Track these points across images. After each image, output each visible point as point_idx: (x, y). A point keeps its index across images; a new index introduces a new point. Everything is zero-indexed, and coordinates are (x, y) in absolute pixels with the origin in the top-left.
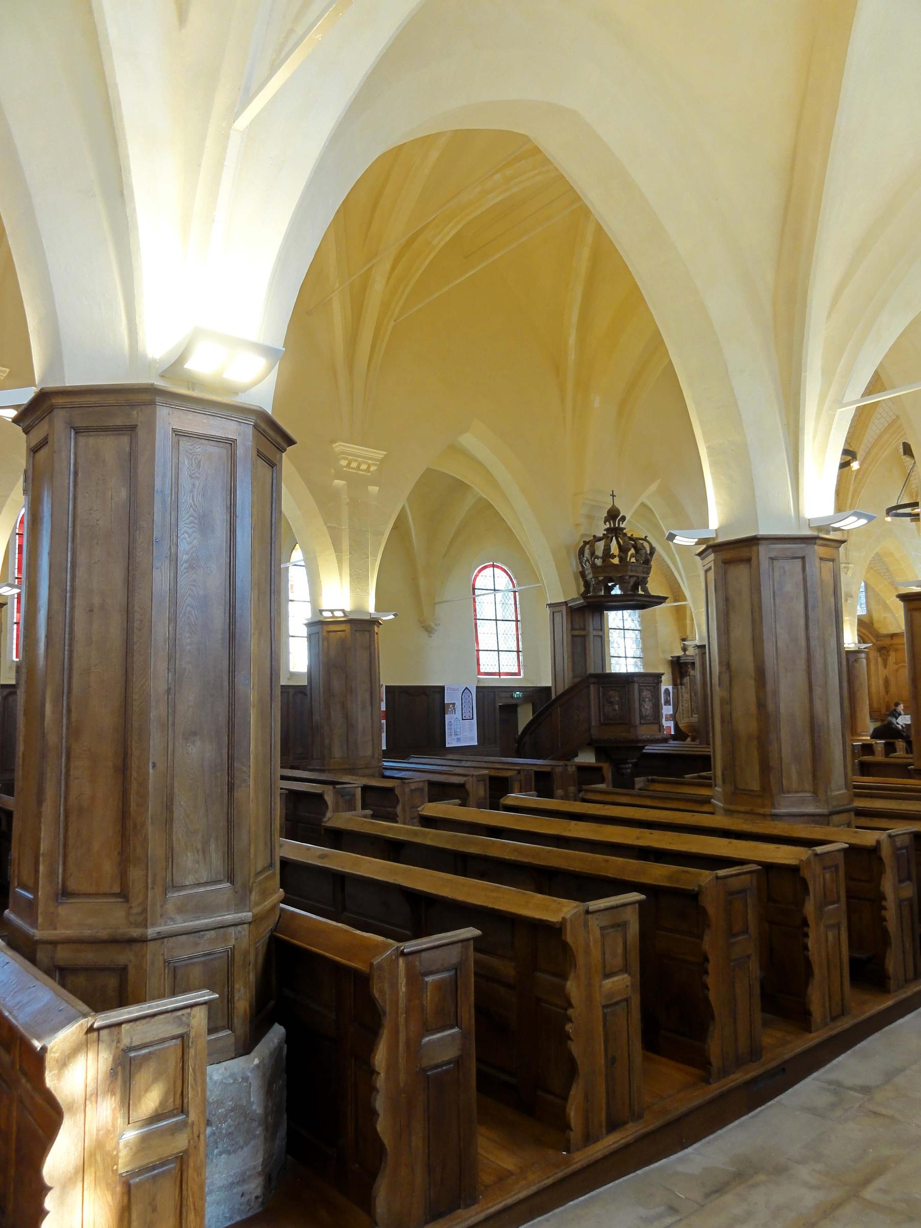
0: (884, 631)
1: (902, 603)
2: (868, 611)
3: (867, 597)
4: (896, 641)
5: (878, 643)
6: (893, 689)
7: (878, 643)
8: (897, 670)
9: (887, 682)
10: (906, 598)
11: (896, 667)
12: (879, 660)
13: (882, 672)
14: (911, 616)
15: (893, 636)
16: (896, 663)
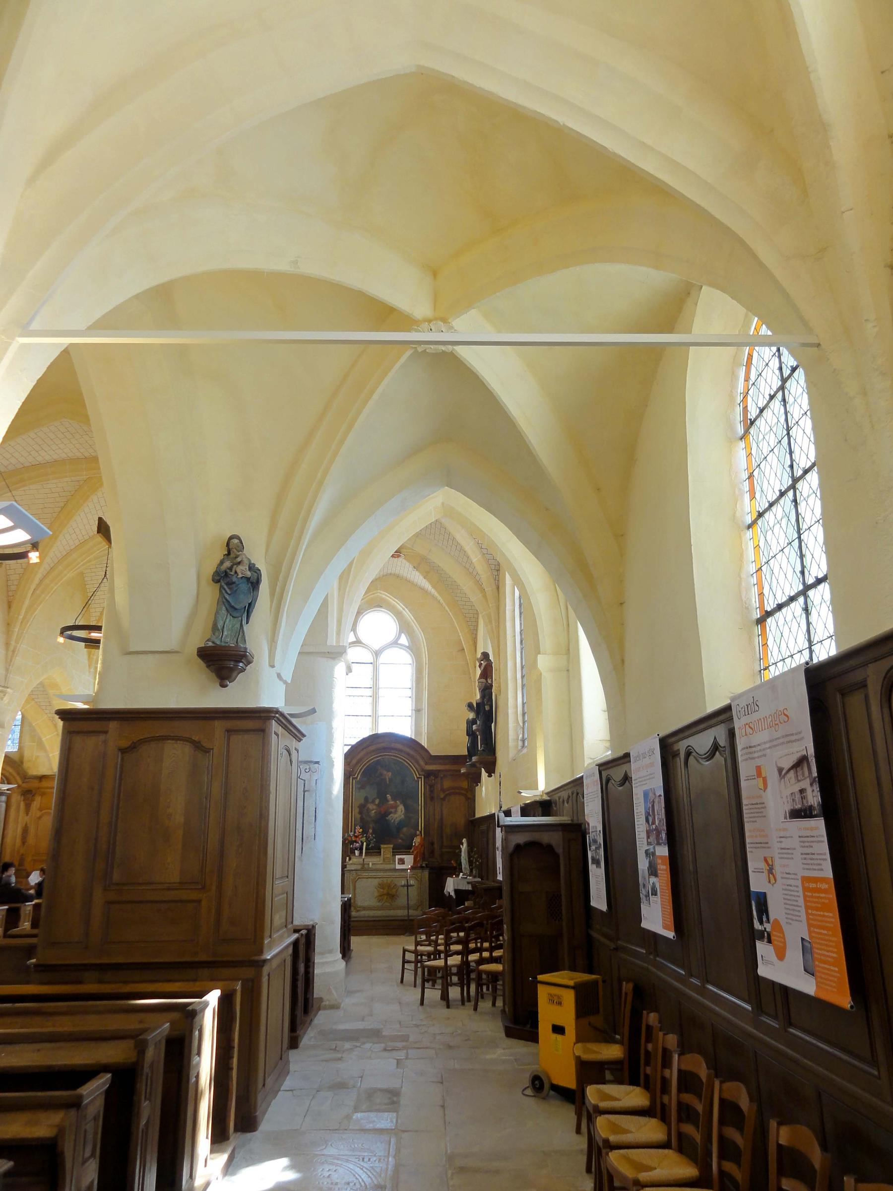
0: (34, 772)
1: (60, 723)
2: (20, 748)
3: (21, 732)
4: (44, 784)
5: (24, 785)
6: (31, 840)
7: (24, 785)
8: (40, 818)
9: (25, 831)
10: (66, 715)
11: (39, 814)
12: (22, 804)
13: (23, 819)
14: (70, 742)
15: (42, 778)
16: (40, 809)
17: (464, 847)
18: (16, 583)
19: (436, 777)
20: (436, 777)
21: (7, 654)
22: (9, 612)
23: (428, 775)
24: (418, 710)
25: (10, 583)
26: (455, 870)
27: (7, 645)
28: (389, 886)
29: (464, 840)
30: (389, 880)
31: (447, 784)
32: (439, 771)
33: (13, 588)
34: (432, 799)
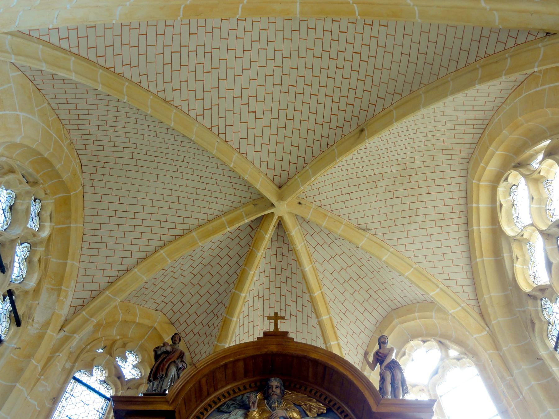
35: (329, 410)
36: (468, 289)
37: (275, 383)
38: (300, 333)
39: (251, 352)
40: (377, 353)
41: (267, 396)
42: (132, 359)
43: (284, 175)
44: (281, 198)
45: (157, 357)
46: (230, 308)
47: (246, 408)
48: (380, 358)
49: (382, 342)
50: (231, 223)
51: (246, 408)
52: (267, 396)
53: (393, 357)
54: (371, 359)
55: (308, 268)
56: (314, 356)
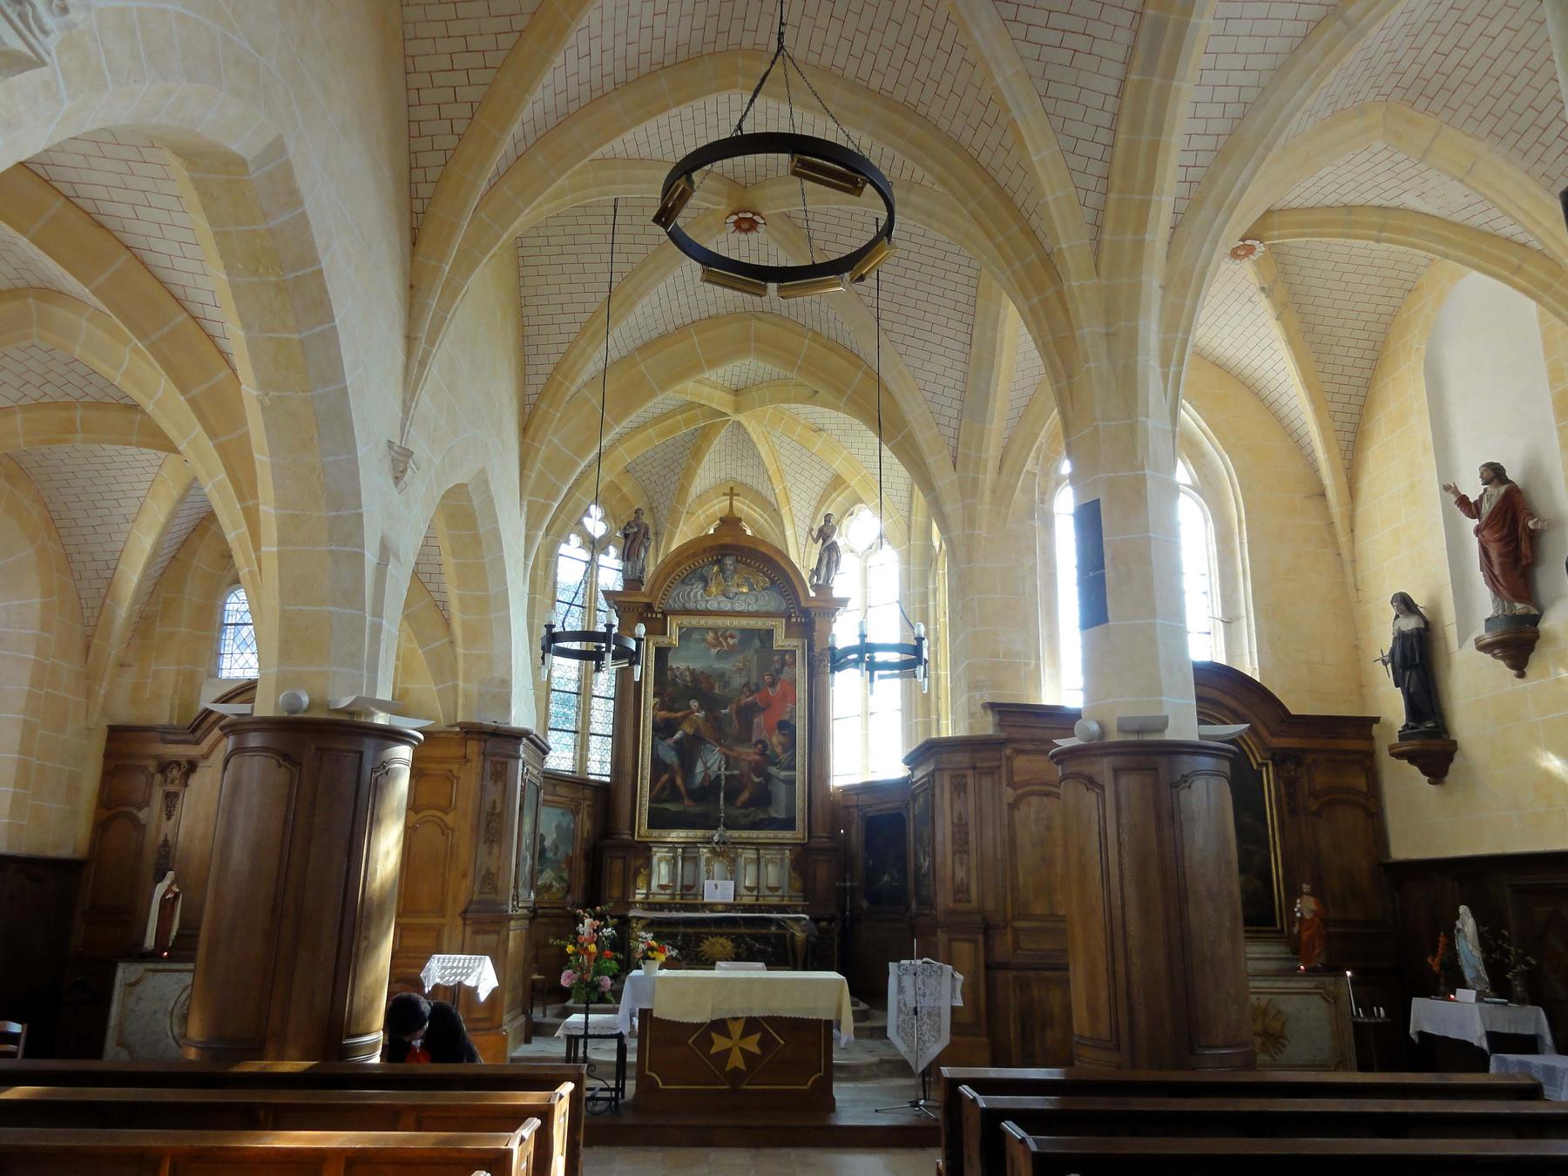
17: (1467, 923)
18: (433, 175)
19: (1299, 763)
20: (1299, 763)
21: (407, 367)
22: (413, 254)
23: (1280, 758)
24: (1229, 621)
25: (418, 175)
26: (1448, 981)
27: (410, 339)
28: (1265, 1012)
29: (1463, 909)
30: (1264, 999)
31: (1322, 780)
32: (1303, 750)
33: (426, 190)
34: (1293, 812)
35: (773, 582)
36: (905, 500)
37: (729, 561)
38: (754, 521)
39: (709, 543)
40: (821, 530)
41: (722, 570)
42: (596, 511)
43: (741, 386)
44: (737, 410)
45: (626, 536)
46: (688, 474)
47: (705, 581)
48: (825, 535)
49: (828, 517)
50: (687, 422)
51: (705, 581)
52: (722, 570)
53: (835, 538)
54: (815, 534)
55: (763, 451)
56: (763, 549)
